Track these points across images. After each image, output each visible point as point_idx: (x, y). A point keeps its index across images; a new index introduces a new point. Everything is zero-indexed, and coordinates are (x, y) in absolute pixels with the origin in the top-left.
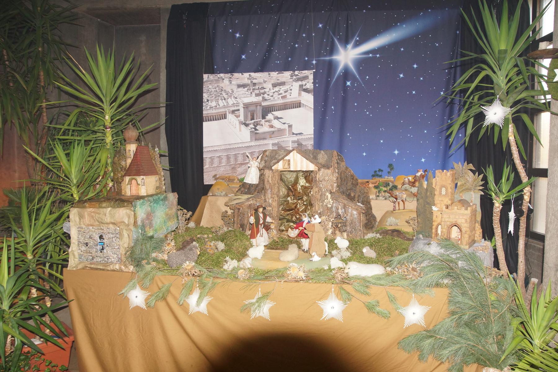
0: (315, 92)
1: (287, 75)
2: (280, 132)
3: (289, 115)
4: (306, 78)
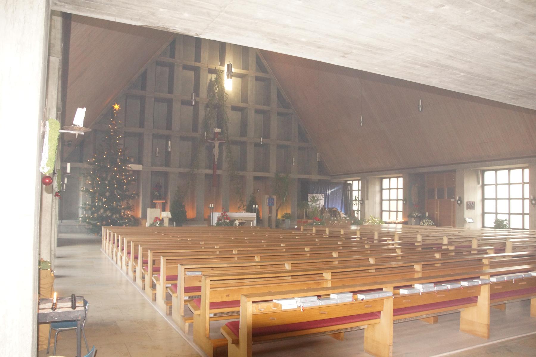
0: (324, 198)
1: (320, 195)
2: (319, 204)
3: (321, 201)
4: (323, 195)
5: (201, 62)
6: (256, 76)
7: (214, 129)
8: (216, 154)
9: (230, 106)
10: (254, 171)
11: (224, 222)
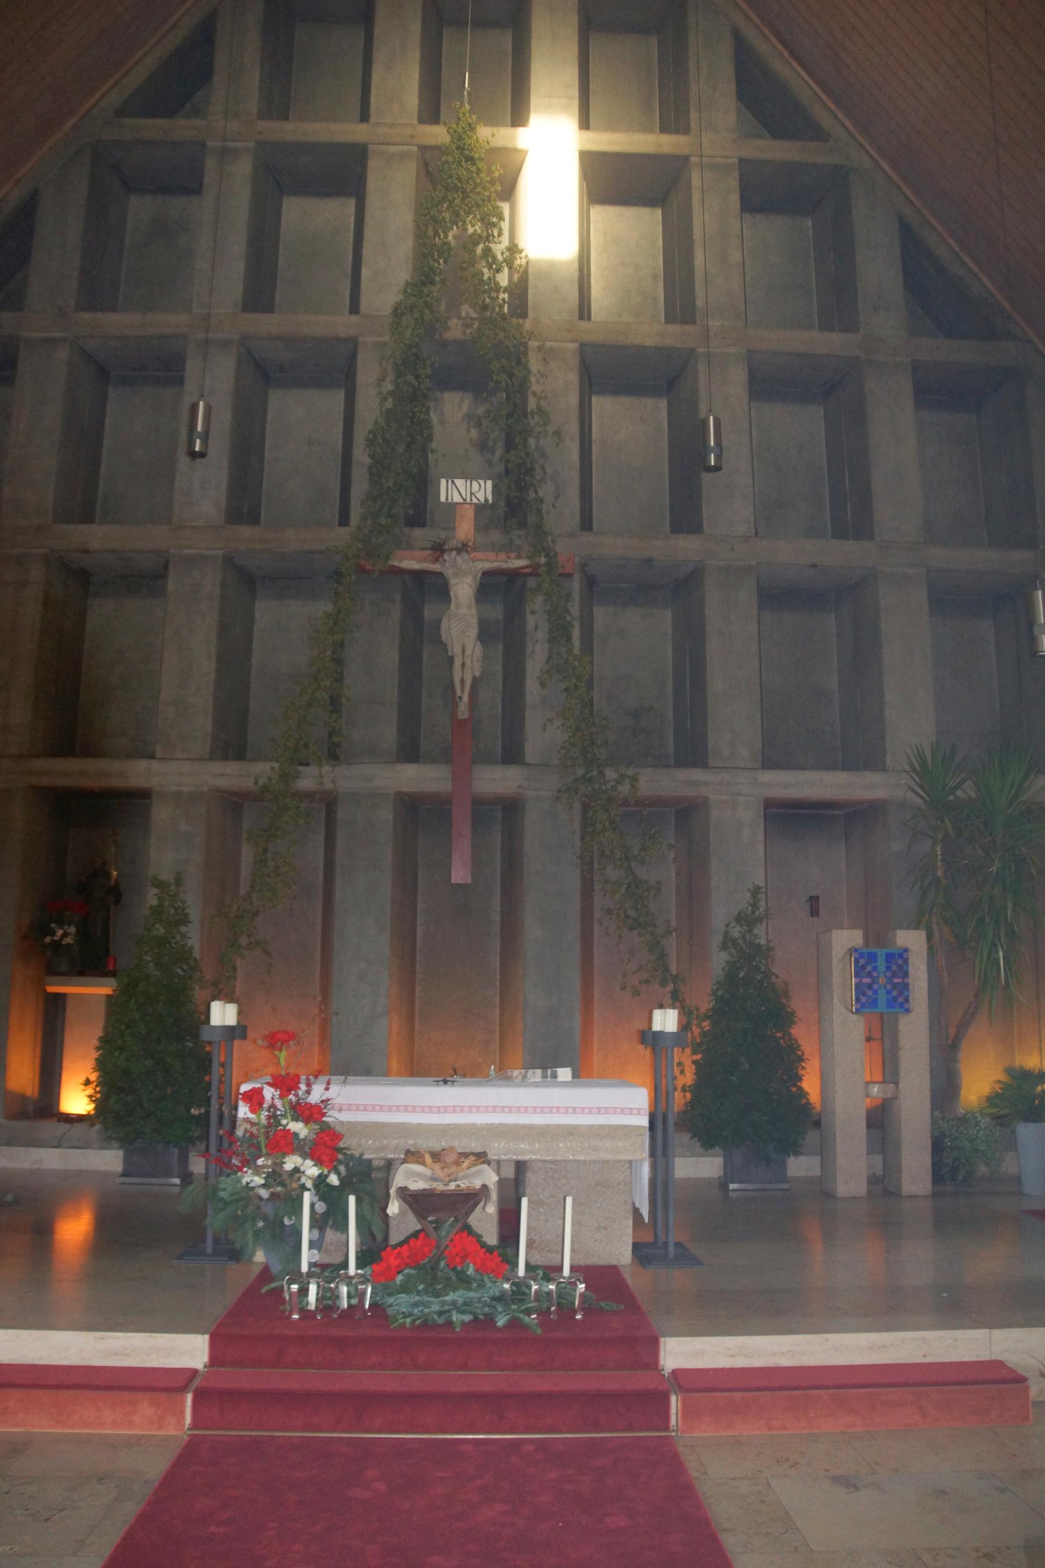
5: (372, 120)
6: (741, 161)
7: (443, 482)
8: (457, 652)
9: (574, 346)
10: (767, 764)
11: (275, 1176)
